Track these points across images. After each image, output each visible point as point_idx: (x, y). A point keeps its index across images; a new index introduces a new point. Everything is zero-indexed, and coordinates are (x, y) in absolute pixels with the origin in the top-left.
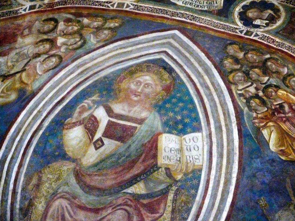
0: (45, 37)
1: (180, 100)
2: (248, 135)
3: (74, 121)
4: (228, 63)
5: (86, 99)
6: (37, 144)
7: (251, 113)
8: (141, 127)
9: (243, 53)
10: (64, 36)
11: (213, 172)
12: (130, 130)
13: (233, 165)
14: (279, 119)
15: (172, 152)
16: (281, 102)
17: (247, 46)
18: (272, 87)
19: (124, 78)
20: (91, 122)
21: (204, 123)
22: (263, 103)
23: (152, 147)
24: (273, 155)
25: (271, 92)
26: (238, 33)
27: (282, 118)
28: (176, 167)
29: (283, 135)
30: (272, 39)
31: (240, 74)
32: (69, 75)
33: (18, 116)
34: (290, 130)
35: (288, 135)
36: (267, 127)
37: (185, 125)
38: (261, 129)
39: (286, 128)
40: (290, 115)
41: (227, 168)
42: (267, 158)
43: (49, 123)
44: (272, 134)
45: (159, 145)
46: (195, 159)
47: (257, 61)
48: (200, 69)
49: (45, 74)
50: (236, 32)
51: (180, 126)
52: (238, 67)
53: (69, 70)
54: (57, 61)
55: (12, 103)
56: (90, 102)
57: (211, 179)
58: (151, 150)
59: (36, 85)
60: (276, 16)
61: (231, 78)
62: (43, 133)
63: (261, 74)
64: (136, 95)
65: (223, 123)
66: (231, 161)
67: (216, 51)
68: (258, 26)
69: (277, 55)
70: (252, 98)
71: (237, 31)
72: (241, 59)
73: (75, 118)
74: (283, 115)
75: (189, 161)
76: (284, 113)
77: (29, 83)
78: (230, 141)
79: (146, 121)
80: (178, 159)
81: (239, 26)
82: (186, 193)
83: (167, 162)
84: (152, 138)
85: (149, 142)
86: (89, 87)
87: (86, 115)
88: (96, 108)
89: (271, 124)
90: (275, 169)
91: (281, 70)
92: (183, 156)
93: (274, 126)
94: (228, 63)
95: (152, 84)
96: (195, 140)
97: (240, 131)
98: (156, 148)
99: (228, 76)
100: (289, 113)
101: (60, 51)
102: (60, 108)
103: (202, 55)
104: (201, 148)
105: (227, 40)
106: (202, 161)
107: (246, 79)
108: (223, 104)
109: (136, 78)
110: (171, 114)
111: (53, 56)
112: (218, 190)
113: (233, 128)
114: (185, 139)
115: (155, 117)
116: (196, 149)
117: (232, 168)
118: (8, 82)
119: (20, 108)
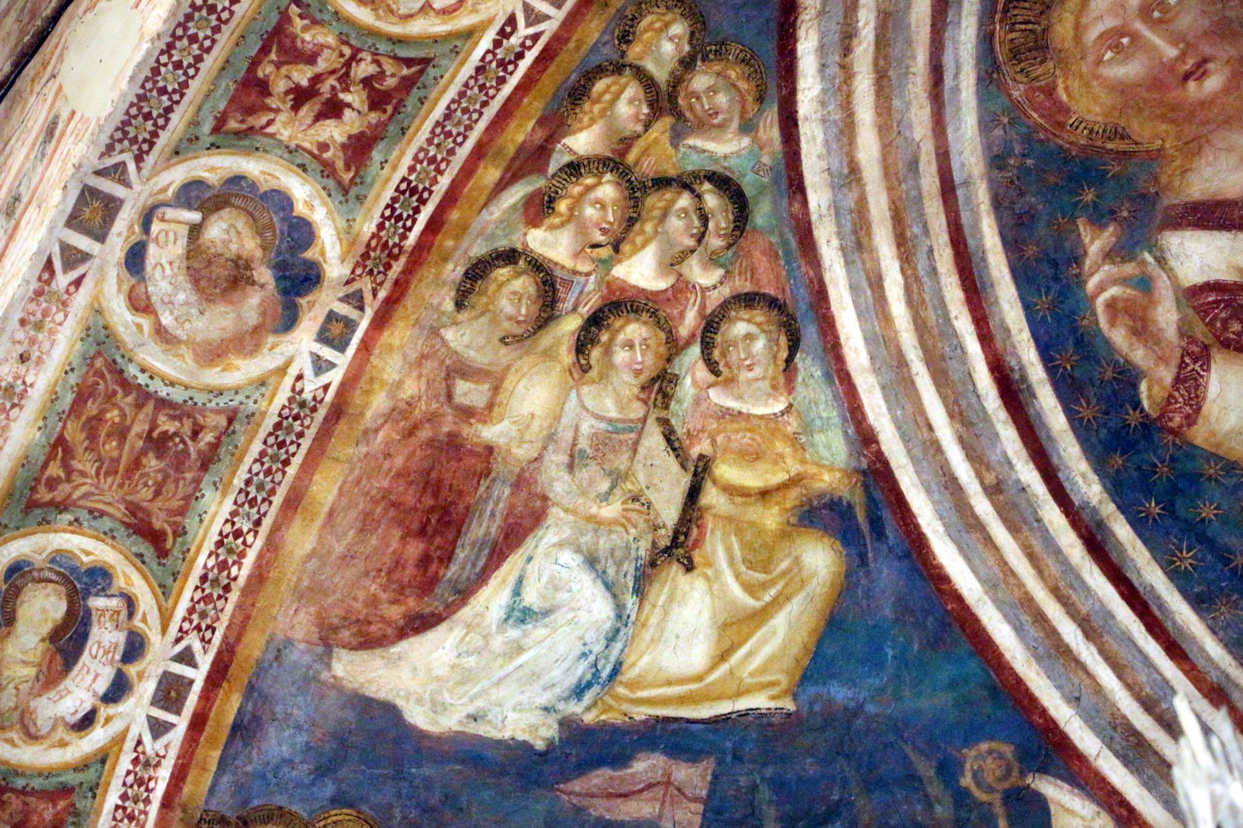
0: (570, 325)
3: (1167, 375)
5: (1080, 282)
6: (1175, 575)
10: (626, 248)
19: (1050, 91)
20: (1223, 315)
32: (881, 299)
33: (939, 578)
43: (1093, 477)
49: (800, 390)
53: (854, 288)
54: (760, 319)
55: (849, 574)
56: (1107, 269)
59: (833, 447)
62: (1138, 524)
64: (1199, 71)
73: (1157, 365)
77: (794, 468)
86: (1012, 245)
87: (1167, 316)
88: (1161, 261)
101: (704, 290)
102: (1047, 403)
109: (1078, 39)
111: (711, 325)
118: (717, 547)
119: (907, 555)
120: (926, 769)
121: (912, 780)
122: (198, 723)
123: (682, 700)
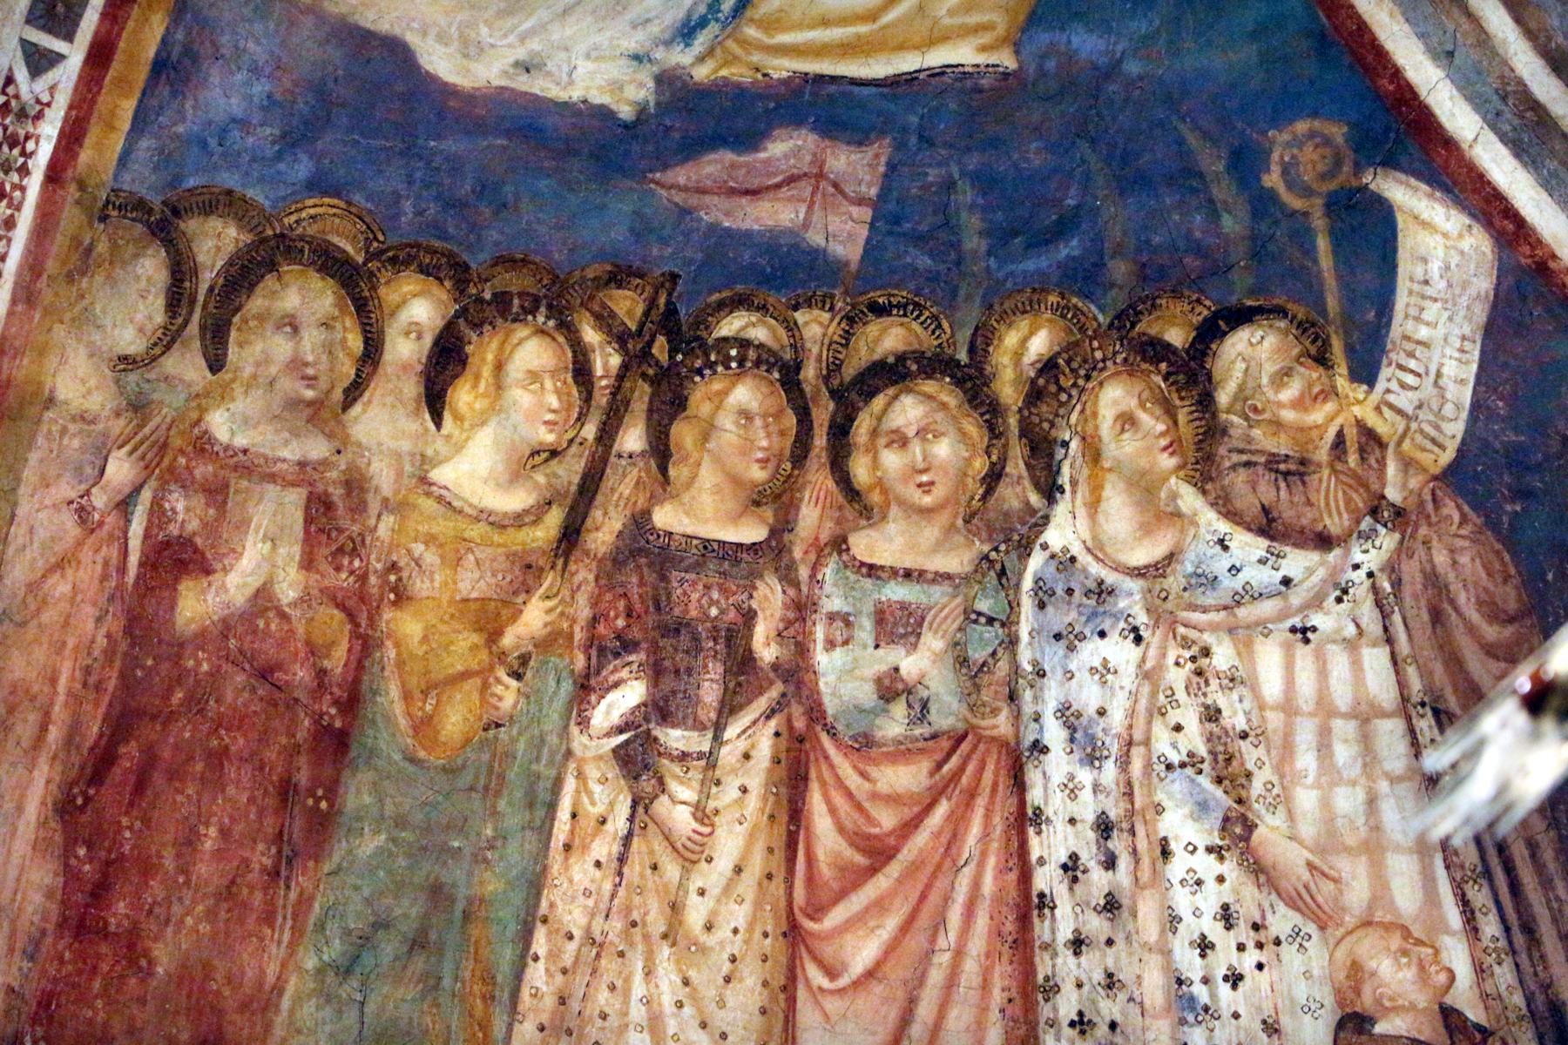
120: (1213, 163)
121: (1188, 177)
122: (100, 55)
123: (847, 49)
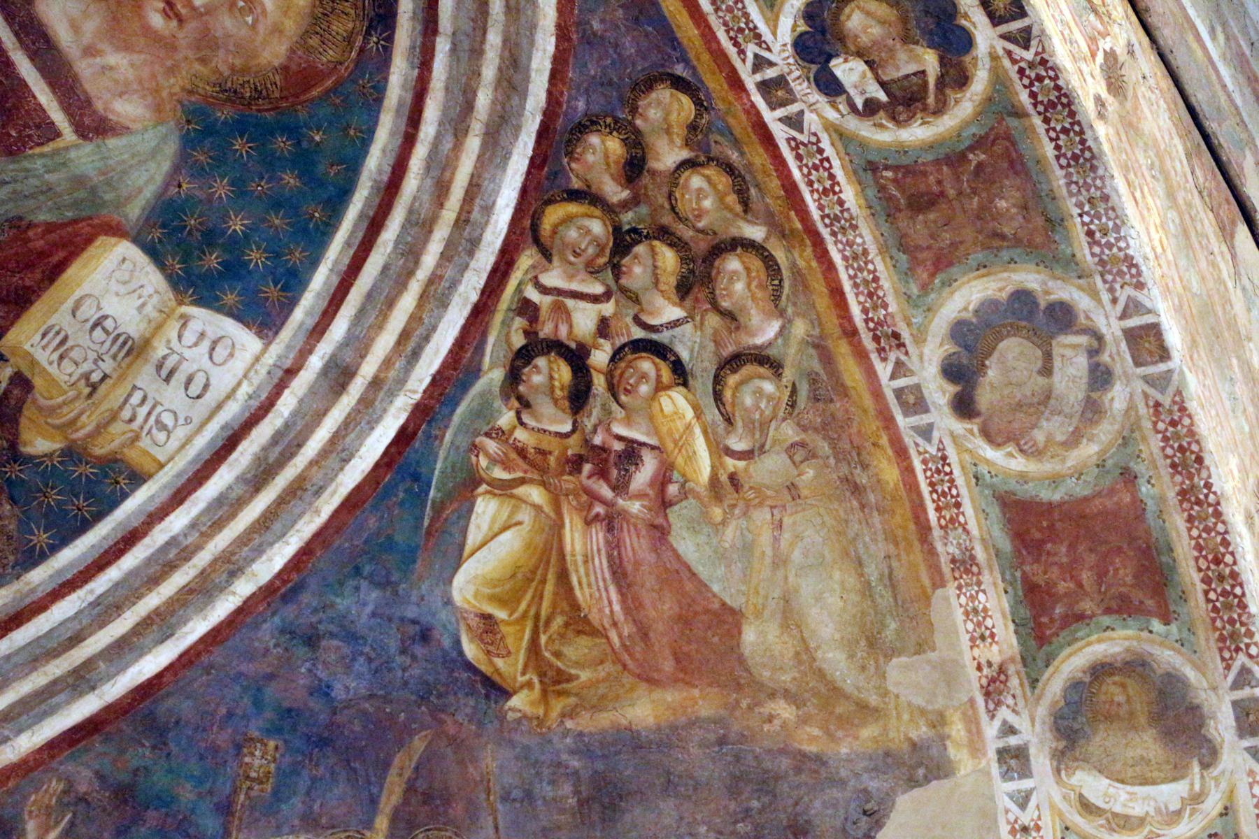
1: (304, 160)
2: (416, 477)
4: (603, 148)
7: (498, 403)
8: (77, 146)
9: (685, 154)
11: (178, 521)
12: (26, 126)
13: (271, 544)
14: (576, 496)
15: (98, 333)
16: (642, 438)
17: (719, 138)
18: (664, 358)
21: (308, 313)
22: (578, 397)
23: (42, 255)
24: (443, 615)
25: (644, 377)
26: (744, 61)
27: (595, 497)
28: (60, 400)
29: (548, 561)
30: (832, 177)
31: (597, 227)
34: (586, 562)
35: (563, 576)
36: (512, 496)
37: (234, 269)
38: (484, 487)
39: (578, 547)
40: (635, 507)
41: (243, 540)
42: (411, 612)
44: (507, 535)
45: (71, 272)
46: (158, 421)
47: (700, 225)
48: (483, 100)
50: (742, 52)
51: (213, 260)
52: (615, 192)
57: (147, 540)
58: (30, 266)
60: (931, 100)
61: (553, 215)
63: (670, 281)
65: (368, 369)
66: (277, 526)
67: (605, 68)
68: (830, 87)
69: (789, 250)
70: (555, 346)
71: (751, 49)
72: (653, 173)
74: (606, 492)
75: (126, 414)
76: (620, 487)
78: (339, 451)
79: (112, 142)
80: (95, 377)
81: (774, 34)
82: (11, 527)
83: (42, 357)
84: (75, 222)
85: (50, 228)
89: (535, 494)
90: (404, 670)
91: (755, 317)
92: (122, 378)
93: (538, 508)
94: (603, 148)
95: (264, 12)
96: (221, 353)
97: (403, 437)
98: (58, 269)
99: (550, 202)
100: (640, 496)
103: (545, 47)
104: (211, 398)
105: (685, 60)
106: (175, 452)
107: (602, 261)
108: (436, 295)
110: (221, 189)
112: (139, 598)
113: (392, 410)
114: (185, 320)
115: (153, 154)
116: (195, 389)
117: (259, 551)
